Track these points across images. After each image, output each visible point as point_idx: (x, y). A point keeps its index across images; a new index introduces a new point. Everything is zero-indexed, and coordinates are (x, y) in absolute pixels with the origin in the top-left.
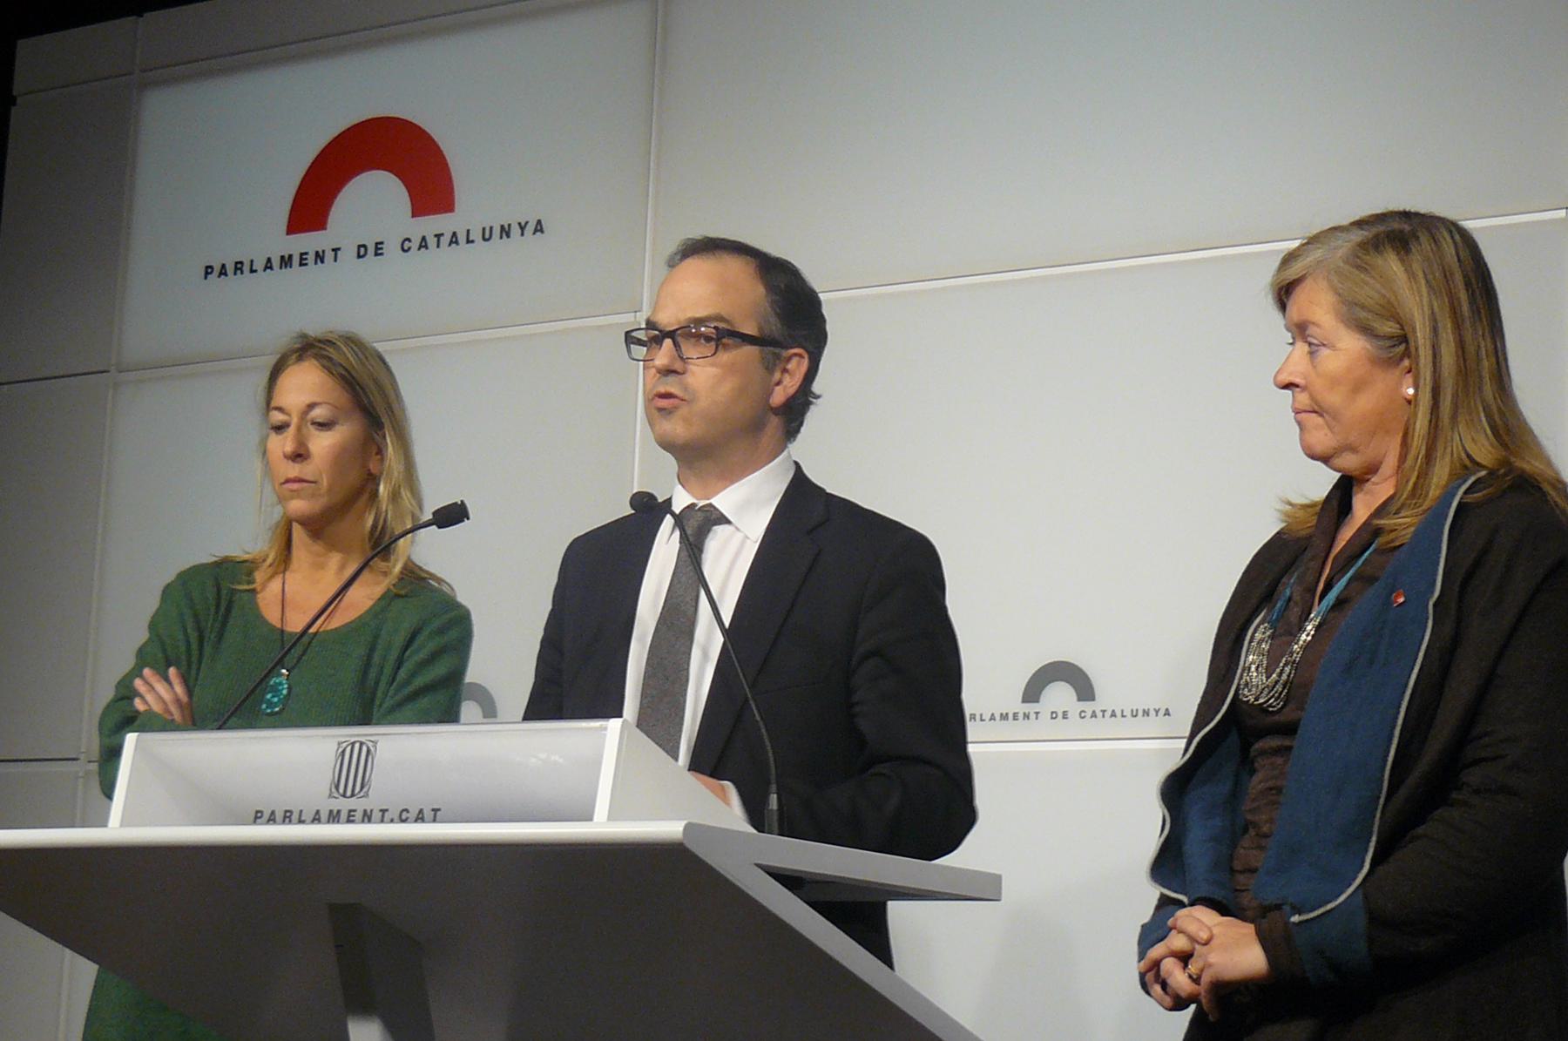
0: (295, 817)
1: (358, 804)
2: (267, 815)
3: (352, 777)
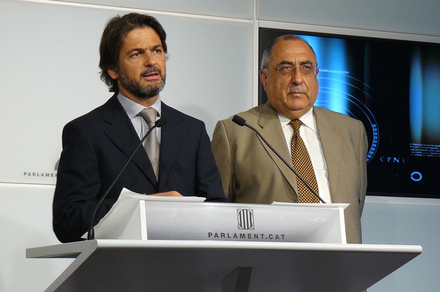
0: (226, 236)
2: (214, 235)
3: (246, 221)
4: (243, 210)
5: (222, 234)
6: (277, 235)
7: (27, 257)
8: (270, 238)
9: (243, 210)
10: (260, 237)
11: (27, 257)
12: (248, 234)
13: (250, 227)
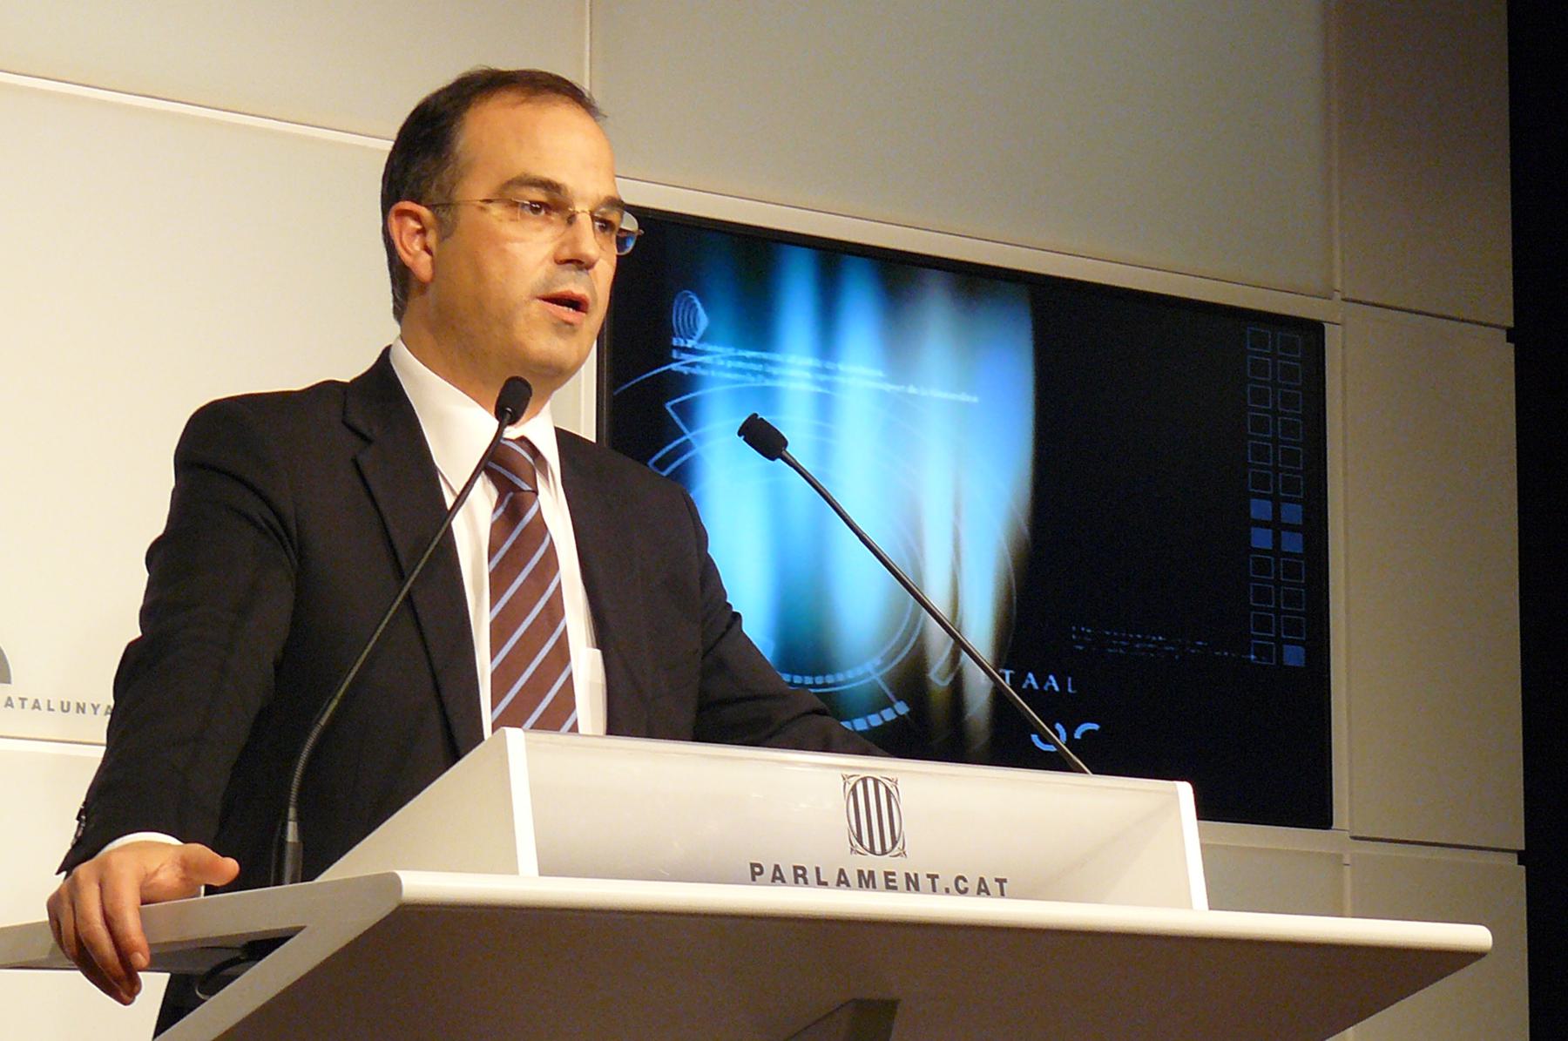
0: (811, 875)
1: (899, 866)
2: (769, 871)
3: (875, 827)
4: (864, 780)
5: (796, 868)
6: (982, 880)
7: (541, 874)
8: (959, 887)
9: (864, 780)
10: (924, 882)
11: (541, 874)
12: (887, 874)
13: (889, 845)
